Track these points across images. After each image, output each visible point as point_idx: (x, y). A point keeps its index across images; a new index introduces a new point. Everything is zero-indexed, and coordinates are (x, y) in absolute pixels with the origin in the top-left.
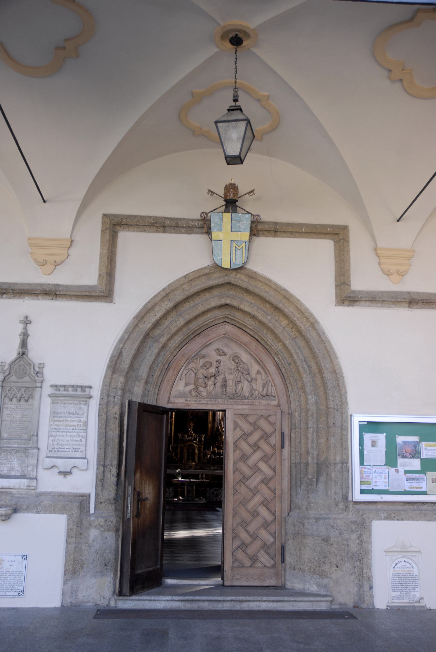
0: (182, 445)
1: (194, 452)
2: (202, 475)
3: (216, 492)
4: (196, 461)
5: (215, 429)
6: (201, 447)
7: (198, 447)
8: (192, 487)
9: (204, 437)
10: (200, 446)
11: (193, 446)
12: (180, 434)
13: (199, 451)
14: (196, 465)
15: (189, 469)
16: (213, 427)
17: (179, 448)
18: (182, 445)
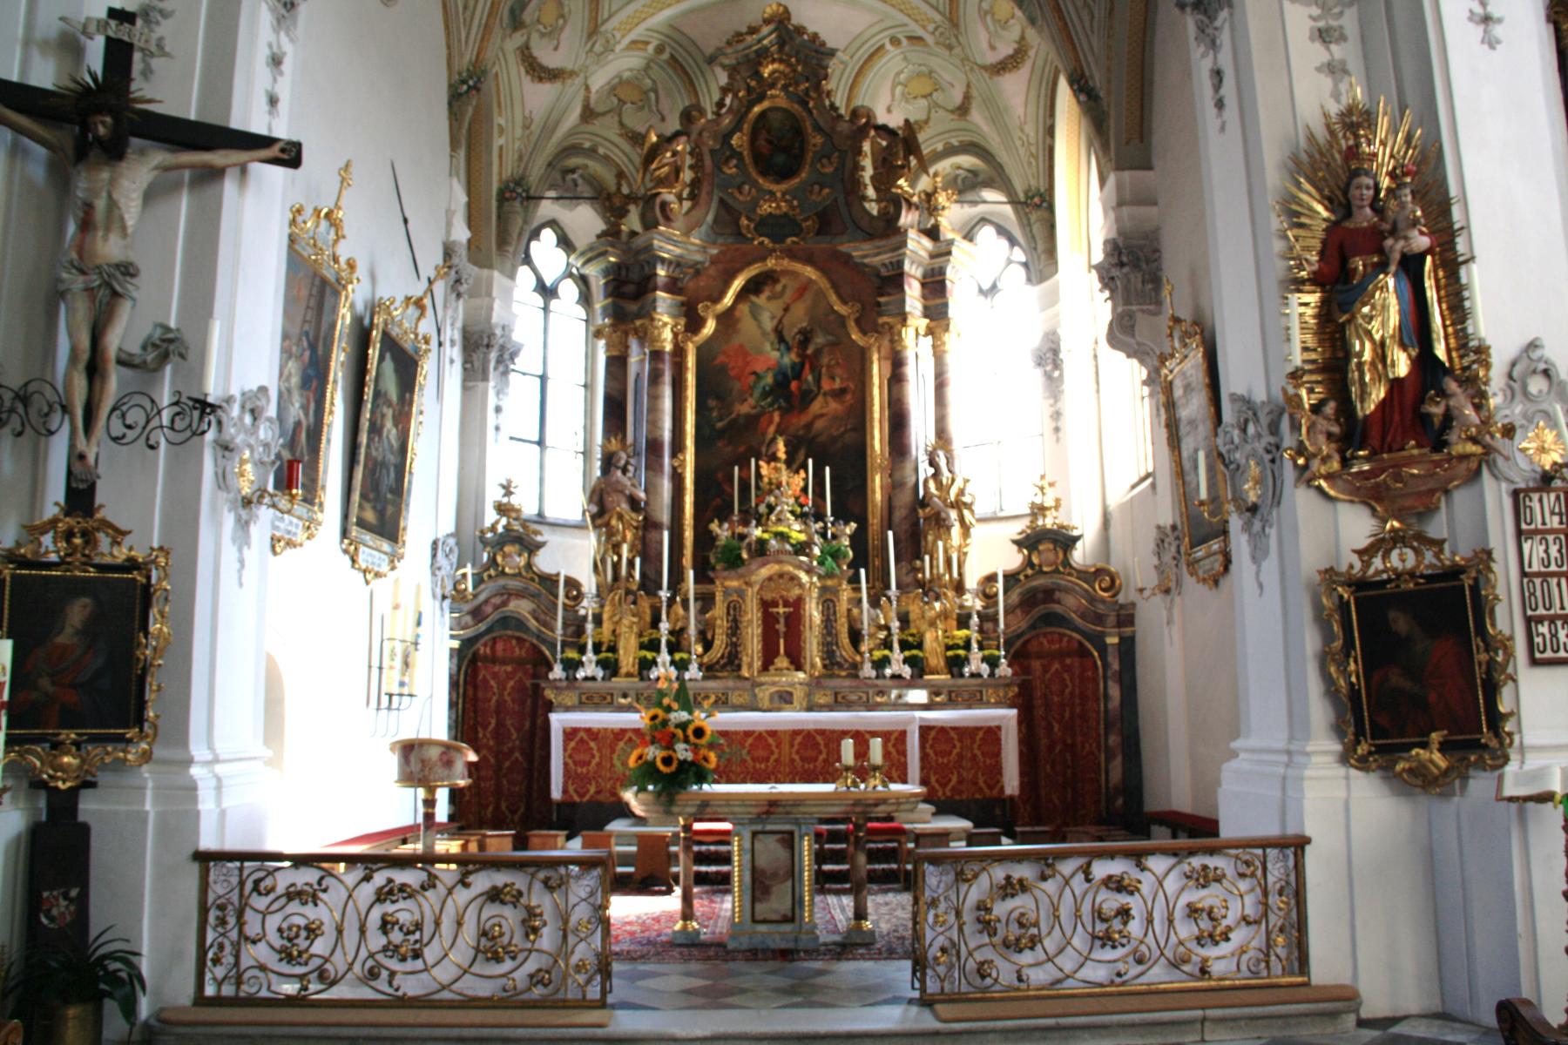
0: (734, 584)
1: (795, 619)
2: (862, 752)
3: (1010, 904)
4: (813, 666)
5: (904, 498)
6: (835, 591)
7: (824, 589)
8: (789, 841)
9: (852, 537)
10: (829, 583)
11: (793, 578)
12: (720, 526)
13: (828, 605)
14: (815, 683)
15: (779, 710)
16: (894, 486)
17: (719, 597)
18: (734, 584)
